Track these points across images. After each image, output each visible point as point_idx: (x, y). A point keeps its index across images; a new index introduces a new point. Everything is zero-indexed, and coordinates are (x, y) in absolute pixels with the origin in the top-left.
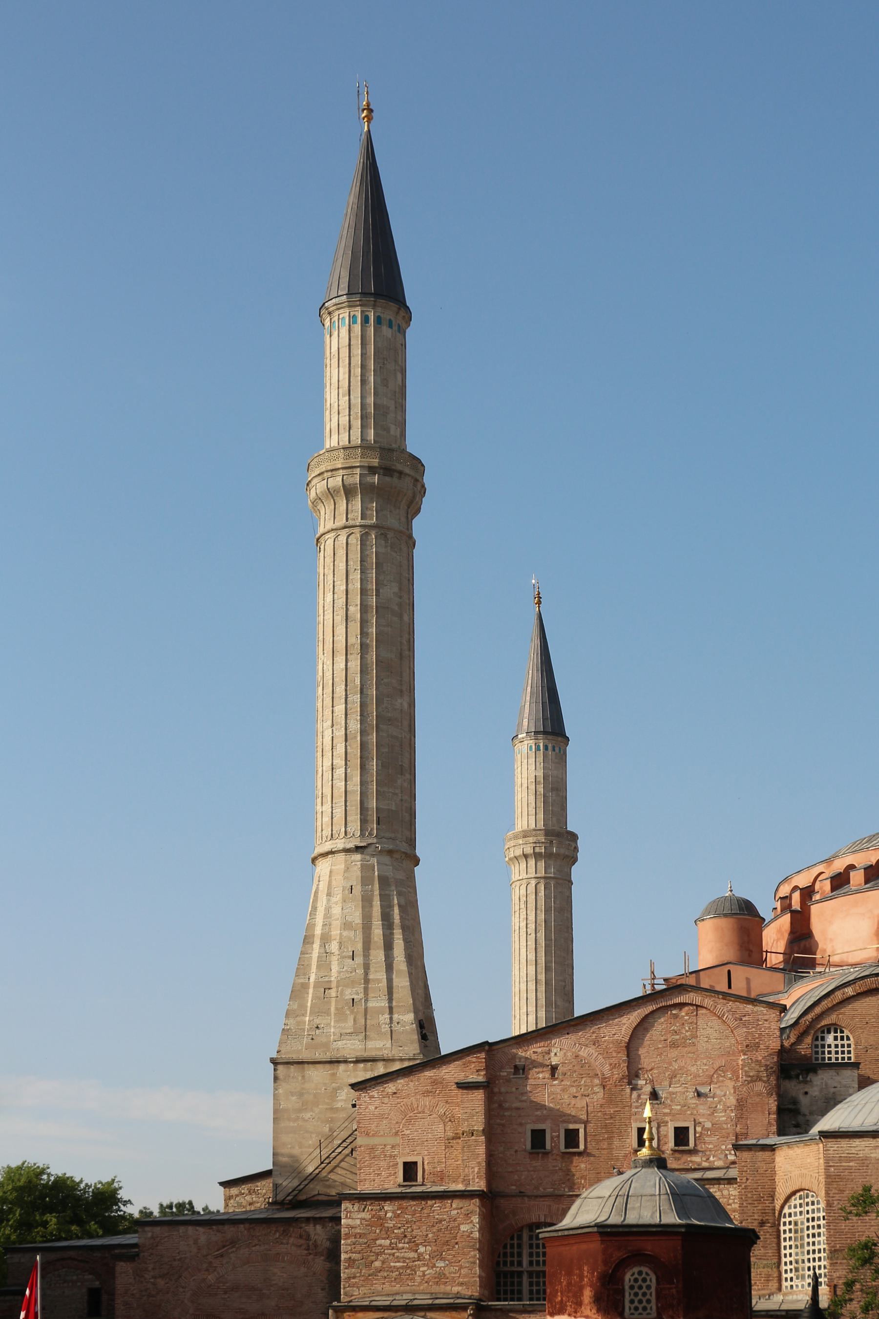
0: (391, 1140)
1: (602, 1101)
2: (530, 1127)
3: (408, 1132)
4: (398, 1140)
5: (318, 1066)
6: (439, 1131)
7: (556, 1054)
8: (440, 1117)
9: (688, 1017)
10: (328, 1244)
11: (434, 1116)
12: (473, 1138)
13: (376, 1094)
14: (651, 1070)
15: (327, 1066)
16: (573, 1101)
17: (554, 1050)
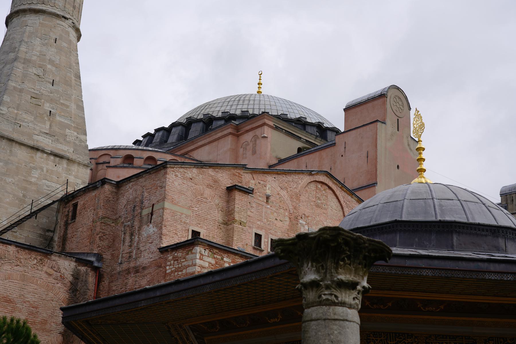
0: (185, 211)
1: (288, 227)
2: (255, 231)
3: (196, 209)
4: (189, 213)
5: (22, 147)
6: (214, 215)
7: (269, 189)
8: (216, 205)
9: (324, 192)
10: (71, 278)
11: (212, 203)
12: (240, 226)
13: (179, 175)
14: (307, 217)
15: (29, 150)
16: (276, 222)
17: (268, 186)
